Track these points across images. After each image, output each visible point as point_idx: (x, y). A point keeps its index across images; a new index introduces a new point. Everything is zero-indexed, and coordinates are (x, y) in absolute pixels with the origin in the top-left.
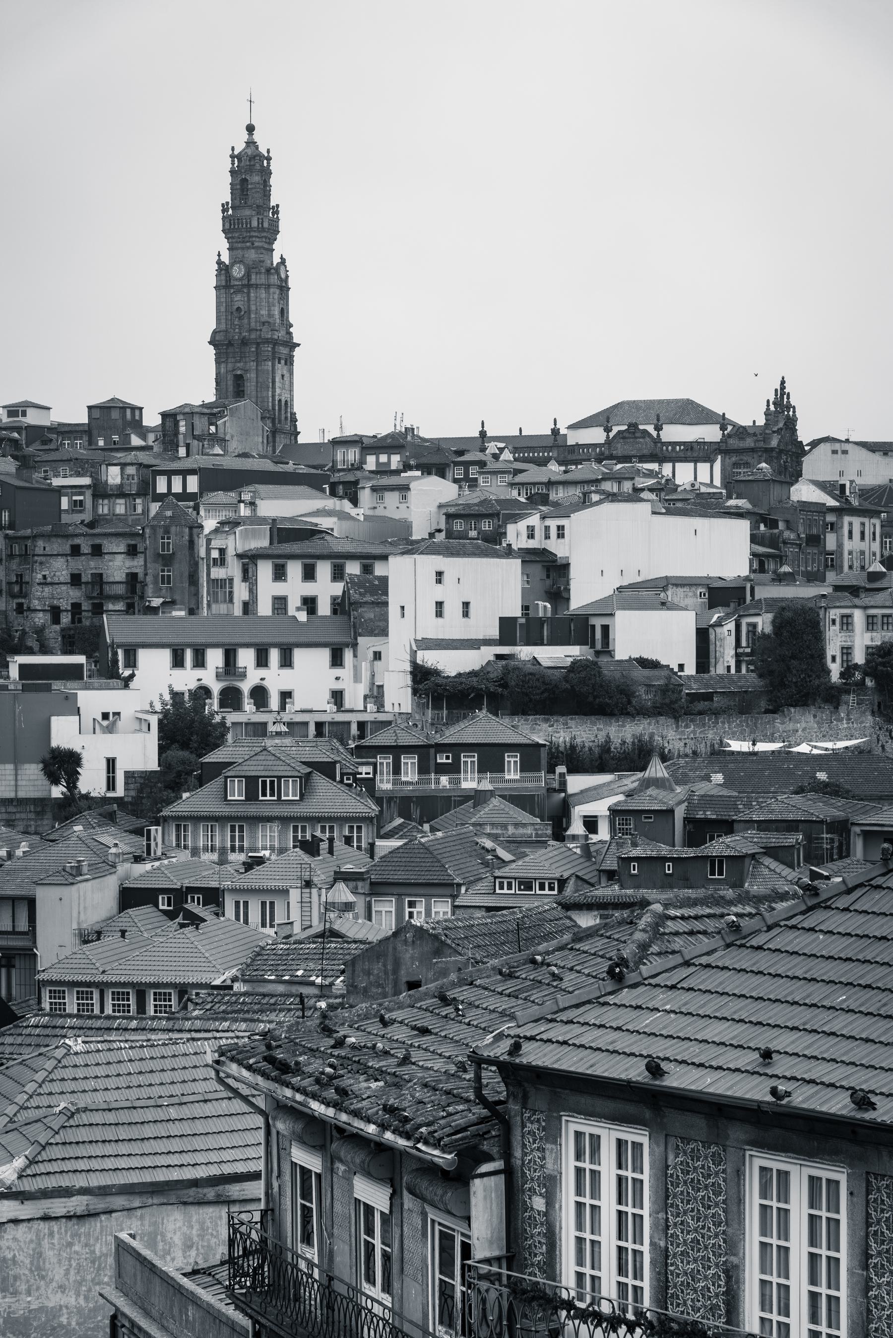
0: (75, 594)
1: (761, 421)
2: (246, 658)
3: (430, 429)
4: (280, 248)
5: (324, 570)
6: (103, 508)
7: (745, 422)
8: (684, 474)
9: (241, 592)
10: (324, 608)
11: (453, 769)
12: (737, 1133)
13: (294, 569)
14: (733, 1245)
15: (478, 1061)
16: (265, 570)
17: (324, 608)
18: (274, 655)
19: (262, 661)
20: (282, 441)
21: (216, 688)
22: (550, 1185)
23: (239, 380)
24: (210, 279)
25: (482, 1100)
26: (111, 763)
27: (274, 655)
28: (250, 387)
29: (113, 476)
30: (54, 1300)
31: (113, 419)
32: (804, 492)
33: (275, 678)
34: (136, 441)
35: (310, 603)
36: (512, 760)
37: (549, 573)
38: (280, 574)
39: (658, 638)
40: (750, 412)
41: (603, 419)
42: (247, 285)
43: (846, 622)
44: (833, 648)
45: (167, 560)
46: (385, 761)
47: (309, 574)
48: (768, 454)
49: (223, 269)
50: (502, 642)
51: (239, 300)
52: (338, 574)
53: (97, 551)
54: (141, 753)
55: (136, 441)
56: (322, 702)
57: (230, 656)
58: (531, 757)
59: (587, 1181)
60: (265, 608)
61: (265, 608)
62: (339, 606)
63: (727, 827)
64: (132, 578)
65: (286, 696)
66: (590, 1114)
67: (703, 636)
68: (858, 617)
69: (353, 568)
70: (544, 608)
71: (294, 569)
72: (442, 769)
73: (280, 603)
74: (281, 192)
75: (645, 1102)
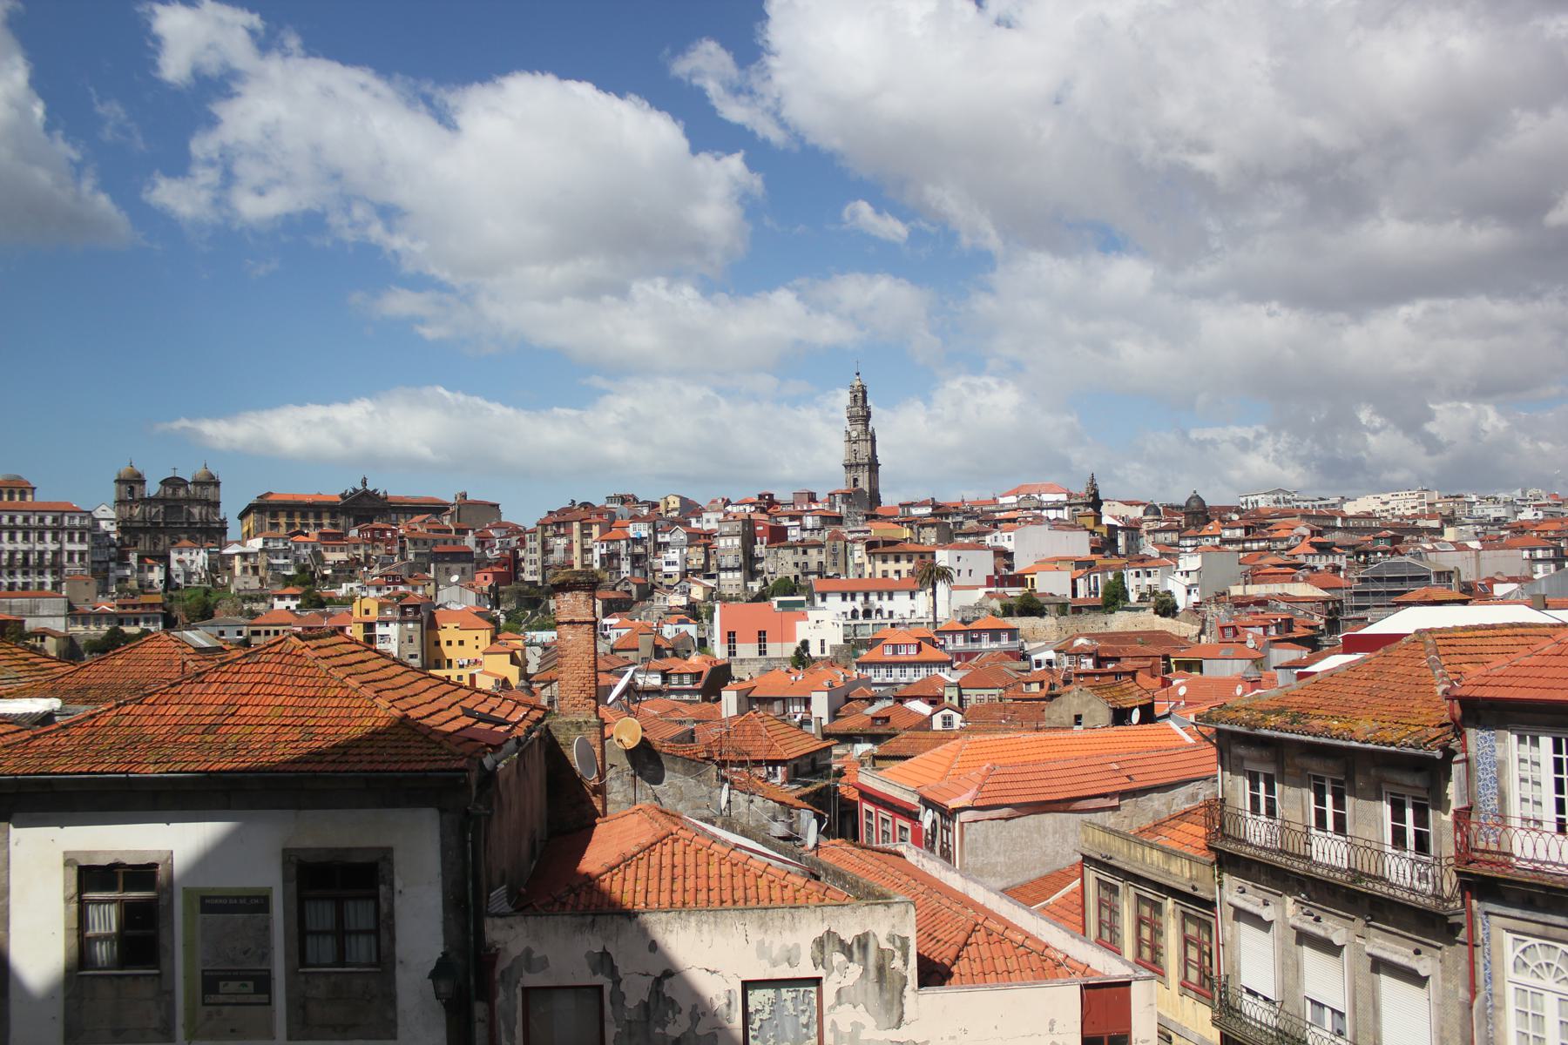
0: (797, 571)
1: (1083, 491)
2: (873, 598)
3: (940, 500)
6: (806, 535)
7: (1075, 491)
8: (1052, 514)
9: (868, 568)
10: (904, 575)
11: (979, 640)
15: (1452, 699)
17: (904, 575)
18: (885, 597)
21: (861, 610)
23: (855, 480)
24: (844, 437)
26: (822, 642)
27: (885, 597)
28: (860, 484)
29: (809, 521)
32: (1106, 520)
33: (886, 605)
34: (814, 507)
35: (898, 572)
36: (1005, 636)
39: (1052, 584)
45: (835, 555)
46: (949, 638)
48: (1087, 505)
50: (989, 585)
51: (855, 446)
52: (910, 561)
53: (805, 552)
54: (836, 637)
55: (814, 507)
56: (907, 615)
57: (867, 596)
58: (1013, 633)
60: (879, 575)
62: (911, 573)
63: (1117, 659)
65: (891, 613)
67: (1074, 582)
69: (916, 558)
70: (1004, 571)
72: (973, 640)
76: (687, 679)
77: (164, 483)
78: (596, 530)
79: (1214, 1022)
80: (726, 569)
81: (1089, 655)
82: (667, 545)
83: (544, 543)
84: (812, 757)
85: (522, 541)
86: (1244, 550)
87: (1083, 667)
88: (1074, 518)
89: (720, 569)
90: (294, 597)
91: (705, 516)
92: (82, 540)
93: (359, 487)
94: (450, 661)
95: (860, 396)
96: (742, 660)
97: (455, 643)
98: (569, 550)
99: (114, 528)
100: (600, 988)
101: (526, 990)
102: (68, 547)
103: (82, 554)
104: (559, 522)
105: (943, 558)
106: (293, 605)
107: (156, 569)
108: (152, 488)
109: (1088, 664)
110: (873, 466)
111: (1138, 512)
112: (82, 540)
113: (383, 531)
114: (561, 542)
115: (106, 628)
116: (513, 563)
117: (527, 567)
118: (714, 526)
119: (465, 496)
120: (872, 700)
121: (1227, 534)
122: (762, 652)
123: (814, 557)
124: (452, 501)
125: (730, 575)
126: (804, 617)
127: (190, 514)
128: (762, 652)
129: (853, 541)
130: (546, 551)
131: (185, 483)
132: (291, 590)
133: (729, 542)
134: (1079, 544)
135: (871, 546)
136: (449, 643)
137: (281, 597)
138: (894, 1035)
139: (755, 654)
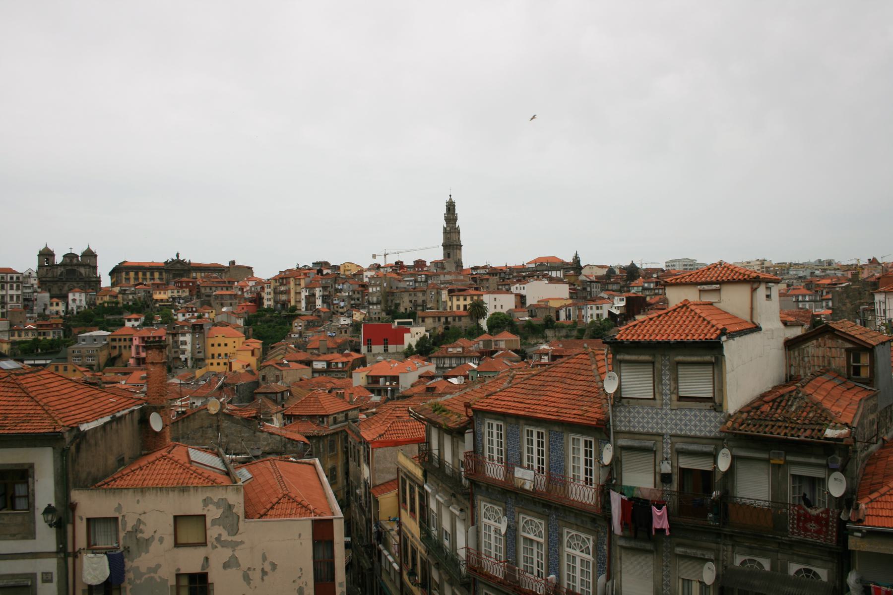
0: (411, 305)
4: (458, 223)
5: (468, 298)
6: (417, 285)
8: (554, 274)
9: (449, 304)
12: (522, 422)
13: (462, 298)
14: (521, 447)
16: (455, 299)
19: (454, 320)
20: (459, 268)
22: (483, 434)
23: (449, 254)
24: (442, 231)
25: (467, 416)
30: (389, 465)
31: (420, 264)
32: (582, 278)
37: (522, 299)
38: (458, 300)
40: (569, 259)
41: (535, 262)
42: (450, 232)
43: (591, 308)
44: (589, 315)
47: (465, 300)
48: (573, 269)
49: (445, 229)
52: (472, 299)
53: (415, 295)
57: (447, 319)
59: (490, 434)
60: (455, 309)
61: (455, 309)
63: (561, 357)
64: (423, 301)
66: (491, 418)
68: (594, 307)
71: (462, 298)
73: (458, 307)
74: (458, 210)
75: (502, 416)
76: (340, 365)
77: (64, 256)
78: (303, 283)
79: (422, 540)
80: (373, 304)
81: (547, 354)
82: (341, 291)
83: (275, 289)
84: (346, 413)
85: (263, 288)
86: (656, 294)
87: (543, 361)
88: (565, 276)
89: (370, 303)
90: (136, 320)
91: (365, 274)
92: (18, 289)
93: (175, 258)
94: (220, 355)
95: (451, 207)
96: (374, 355)
97: (223, 345)
98: (287, 292)
99: (36, 282)
100: (117, 518)
101: (88, 520)
102: (10, 292)
103: (18, 296)
104: (283, 278)
105: (487, 298)
106: (136, 324)
107: (60, 304)
108: (58, 260)
109: (545, 360)
110: (459, 246)
111: (603, 272)
112: (18, 289)
113: (187, 283)
114: (283, 288)
115: (30, 337)
116: (258, 300)
117: (266, 304)
118: (366, 280)
119: (233, 263)
120: (432, 378)
121: (646, 285)
122: (386, 350)
123: (420, 298)
124: (227, 265)
125: (375, 307)
126: (408, 331)
127: (81, 274)
128: (386, 350)
129: (442, 289)
130: (276, 292)
131: (78, 256)
132: (135, 316)
133: (374, 289)
134: (562, 292)
135: (451, 292)
136: (219, 345)
137: (129, 320)
138: (235, 538)
139: (383, 351)
